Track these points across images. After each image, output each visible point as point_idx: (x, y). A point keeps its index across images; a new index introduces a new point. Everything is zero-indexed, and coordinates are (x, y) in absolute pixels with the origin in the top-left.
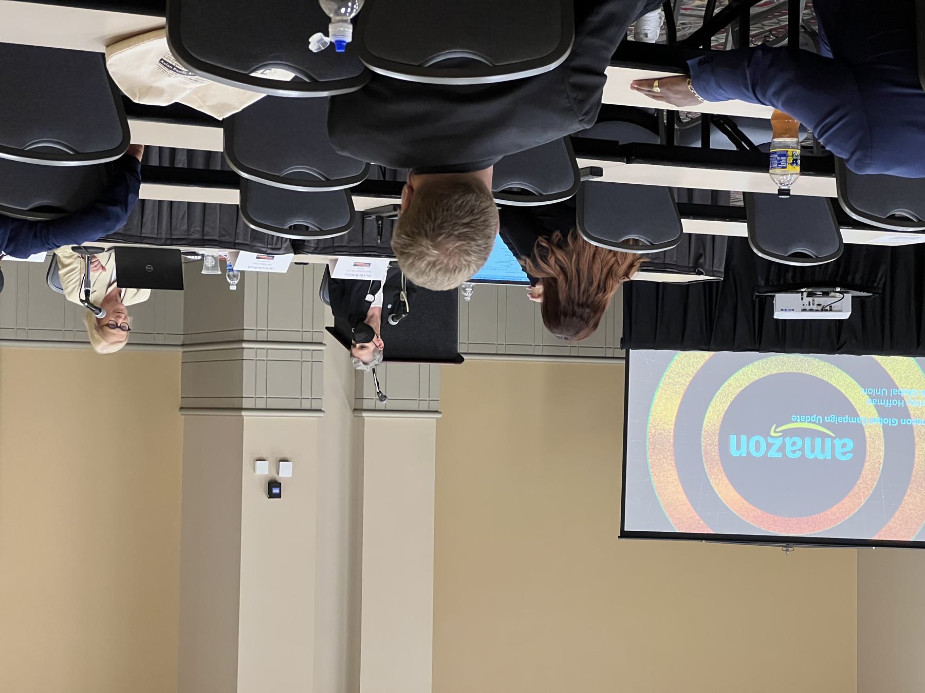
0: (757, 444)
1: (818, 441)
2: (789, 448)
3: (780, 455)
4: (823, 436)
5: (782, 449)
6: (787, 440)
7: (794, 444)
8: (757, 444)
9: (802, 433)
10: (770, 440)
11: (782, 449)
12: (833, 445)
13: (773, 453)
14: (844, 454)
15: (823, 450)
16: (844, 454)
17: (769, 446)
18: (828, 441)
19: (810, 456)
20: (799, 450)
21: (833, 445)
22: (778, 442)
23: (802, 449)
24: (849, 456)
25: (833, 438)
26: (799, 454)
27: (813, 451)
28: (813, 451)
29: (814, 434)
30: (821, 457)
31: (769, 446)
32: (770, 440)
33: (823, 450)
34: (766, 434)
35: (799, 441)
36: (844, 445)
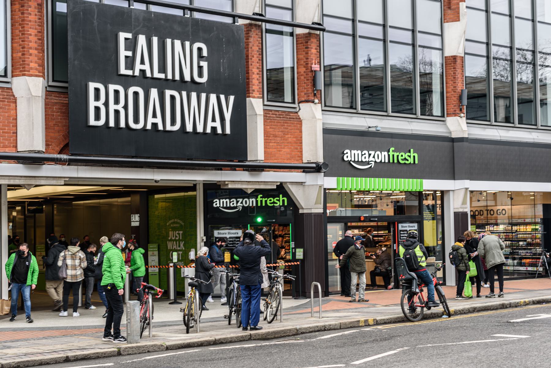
1: (225, 205)
2: (235, 202)
3: (238, 200)
4: (223, 207)
5: (237, 202)
6: (235, 205)
7: (233, 204)
10: (241, 205)
11: (237, 202)
13: (241, 200)
14: (216, 202)
15: (223, 202)
16: (216, 202)
17: (242, 203)
18: (221, 205)
19: (228, 200)
22: (239, 204)
23: (230, 202)
24: (215, 201)
25: (220, 207)
26: (232, 200)
27: (227, 202)
28: (227, 202)
29: (227, 208)
31: (242, 203)
33: (223, 202)
34: (243, 207)
35: (232, 205)
36: (216, 204)
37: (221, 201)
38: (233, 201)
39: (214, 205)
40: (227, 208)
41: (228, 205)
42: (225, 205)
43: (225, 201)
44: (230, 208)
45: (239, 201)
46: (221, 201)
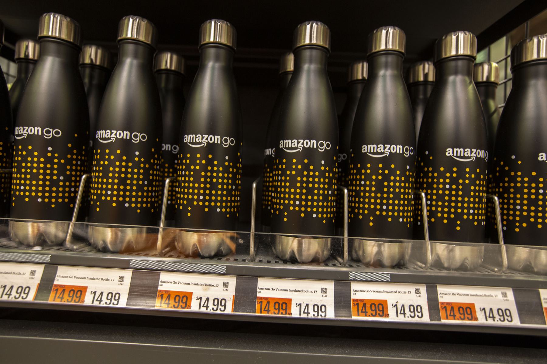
0: (479, 154)
1: (459, 155)
2: (469, 152)
4: (457, 156)
6: (469, 155)
7: (467, 154)
8: (479, 154)
9: (464, 157)
12: (453, 153)
15: (457, 151)
16: (449, 151)
18: (455, 155)
19: (462, 150)
20: (466, 152)
21: (453, 153)
23: (464, 152)
24: (447, 150)
27: (461, 152)
28: (461, 152)
29: (460, 157)
30: (458, 149)
31: (475, 153)
32: (476, 156)
33: (457, 151)
35: (466, 155)
36: (449, 153)
37: (455, 150)
38: (468, 151)
39: (447, 154)
40: (460, 157)
41: (462, 155)
42: (459, 155)
43: (458, 150)
44: (464, 157)
45: (473, 151)
46: (455, 150)
